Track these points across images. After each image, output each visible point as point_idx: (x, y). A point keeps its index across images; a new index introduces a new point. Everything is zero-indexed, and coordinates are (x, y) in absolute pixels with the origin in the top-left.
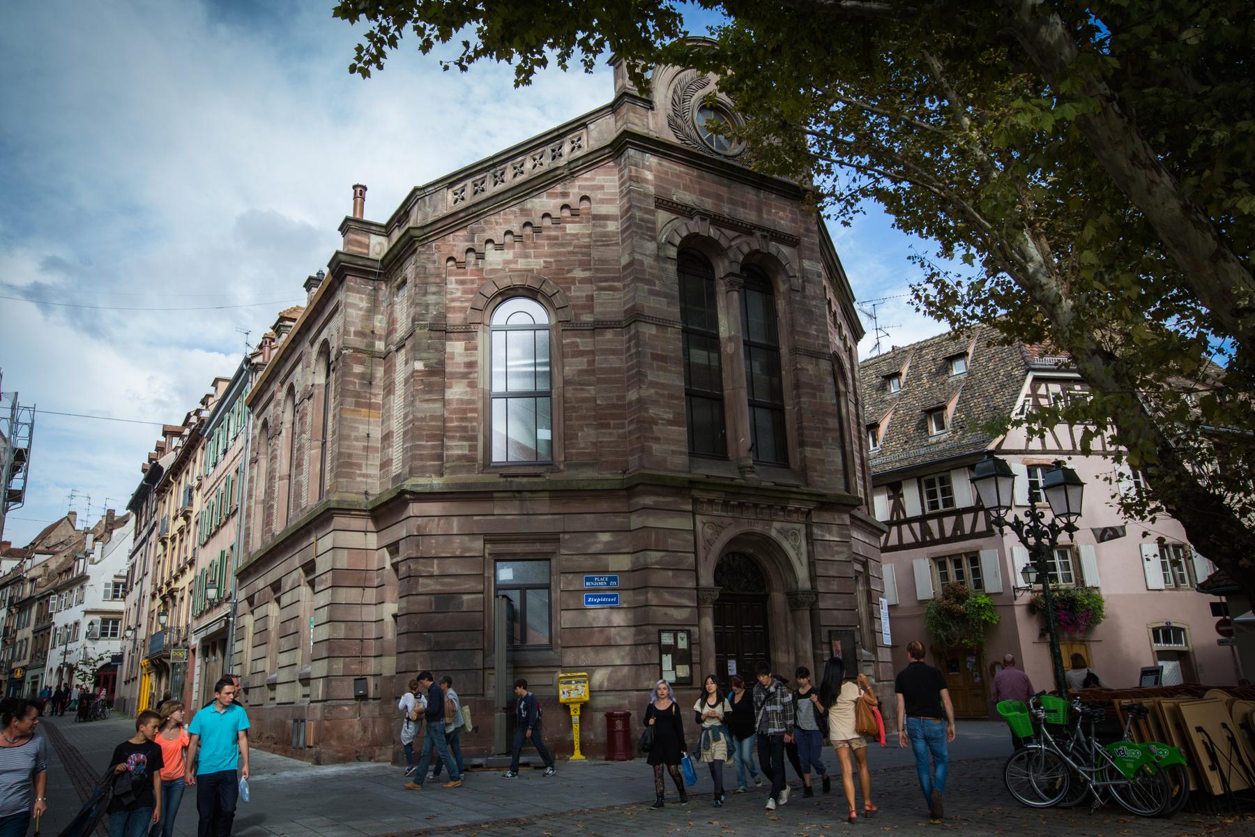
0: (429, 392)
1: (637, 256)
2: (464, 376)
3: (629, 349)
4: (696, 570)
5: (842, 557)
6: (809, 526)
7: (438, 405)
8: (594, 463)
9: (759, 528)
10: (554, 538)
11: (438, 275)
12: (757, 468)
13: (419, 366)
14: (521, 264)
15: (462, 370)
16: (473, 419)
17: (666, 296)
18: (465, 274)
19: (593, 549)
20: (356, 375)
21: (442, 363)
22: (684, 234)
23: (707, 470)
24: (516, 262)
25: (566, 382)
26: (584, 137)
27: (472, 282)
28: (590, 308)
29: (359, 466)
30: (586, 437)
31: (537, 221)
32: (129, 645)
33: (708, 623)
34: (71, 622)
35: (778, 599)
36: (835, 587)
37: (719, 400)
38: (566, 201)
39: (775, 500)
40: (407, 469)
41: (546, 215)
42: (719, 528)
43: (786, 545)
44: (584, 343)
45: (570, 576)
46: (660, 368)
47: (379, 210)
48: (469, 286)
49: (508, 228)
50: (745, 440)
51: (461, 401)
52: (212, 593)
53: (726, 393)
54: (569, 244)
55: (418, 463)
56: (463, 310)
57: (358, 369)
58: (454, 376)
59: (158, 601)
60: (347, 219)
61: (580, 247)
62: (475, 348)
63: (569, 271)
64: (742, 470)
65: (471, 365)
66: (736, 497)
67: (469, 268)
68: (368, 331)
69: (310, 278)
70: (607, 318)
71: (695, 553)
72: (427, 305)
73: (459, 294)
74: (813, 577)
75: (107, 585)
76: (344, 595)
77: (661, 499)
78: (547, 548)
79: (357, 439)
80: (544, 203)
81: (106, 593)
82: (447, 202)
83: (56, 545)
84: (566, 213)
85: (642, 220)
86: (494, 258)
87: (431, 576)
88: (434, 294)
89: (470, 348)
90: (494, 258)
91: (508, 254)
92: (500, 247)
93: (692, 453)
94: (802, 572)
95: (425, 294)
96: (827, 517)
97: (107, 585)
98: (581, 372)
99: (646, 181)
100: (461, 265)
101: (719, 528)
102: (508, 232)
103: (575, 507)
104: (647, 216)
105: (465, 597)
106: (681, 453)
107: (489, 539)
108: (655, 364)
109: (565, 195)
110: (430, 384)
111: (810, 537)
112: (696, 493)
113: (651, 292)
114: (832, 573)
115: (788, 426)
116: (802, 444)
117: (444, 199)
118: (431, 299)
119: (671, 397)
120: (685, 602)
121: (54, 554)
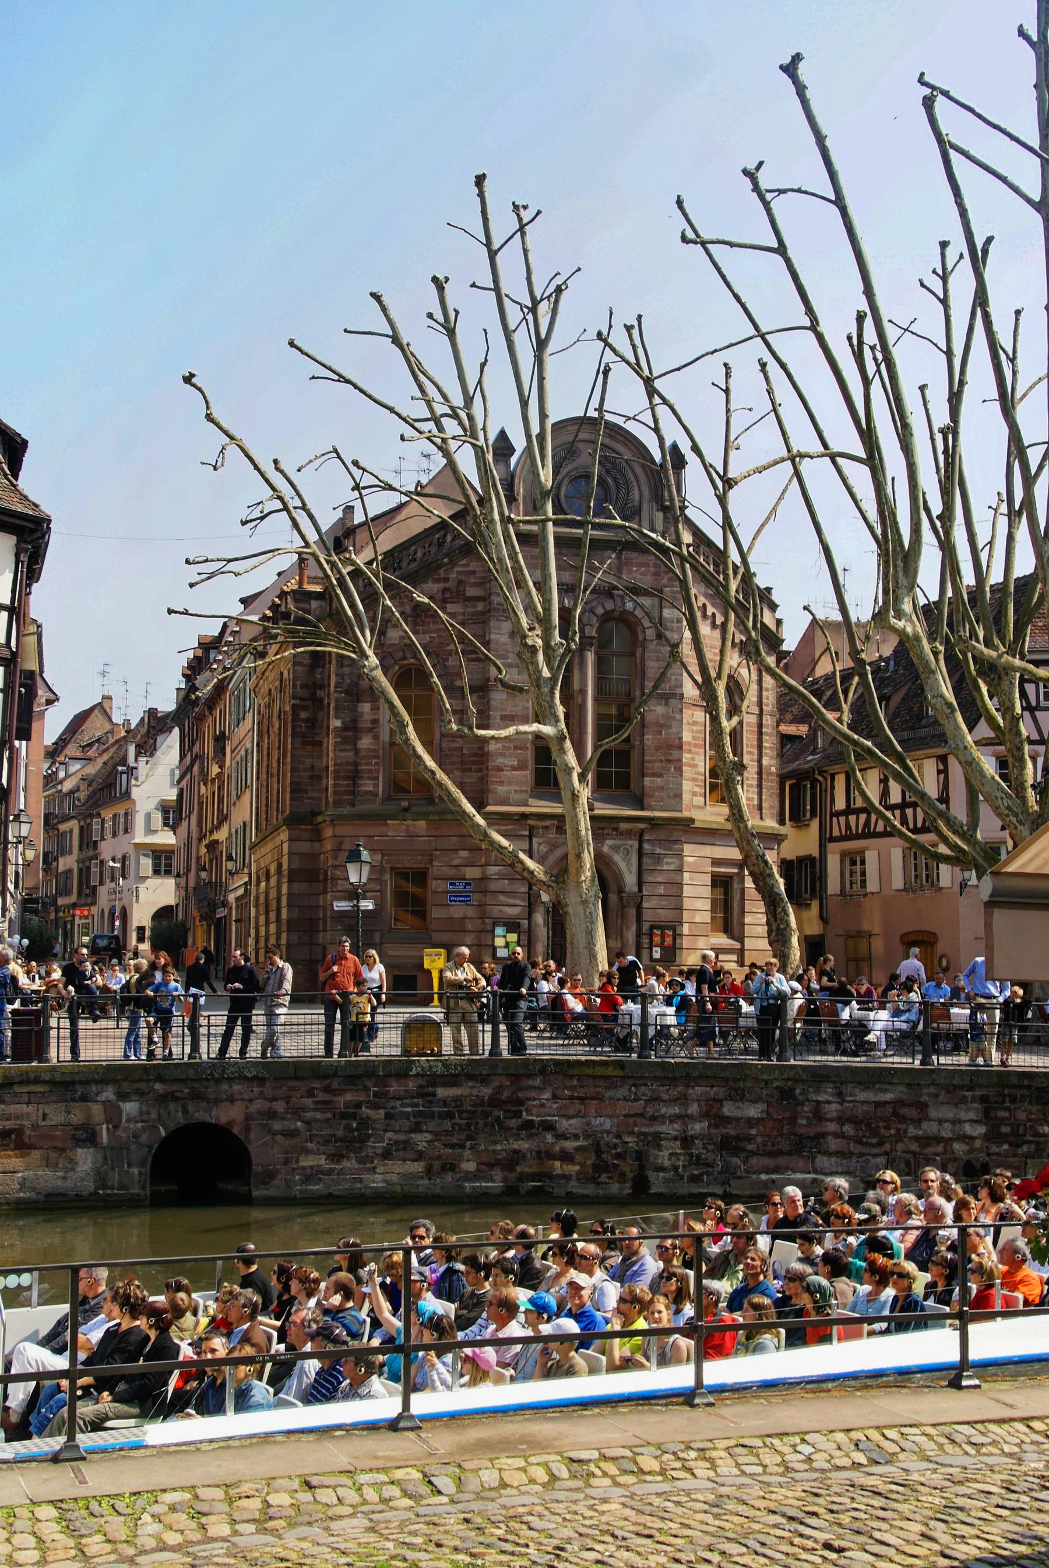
0: (346, 744)
2: (370, 730)
5: (672, 867)
6: (641, 843)
7: (351, 754)
15: (369, 725)
19: (456, 862)
20: (303, 720)
21: (354, 721)
29: (306, 791)
36: (661, 890)
57: (303, 715)
74: (640, 884)
79: (304, 770)
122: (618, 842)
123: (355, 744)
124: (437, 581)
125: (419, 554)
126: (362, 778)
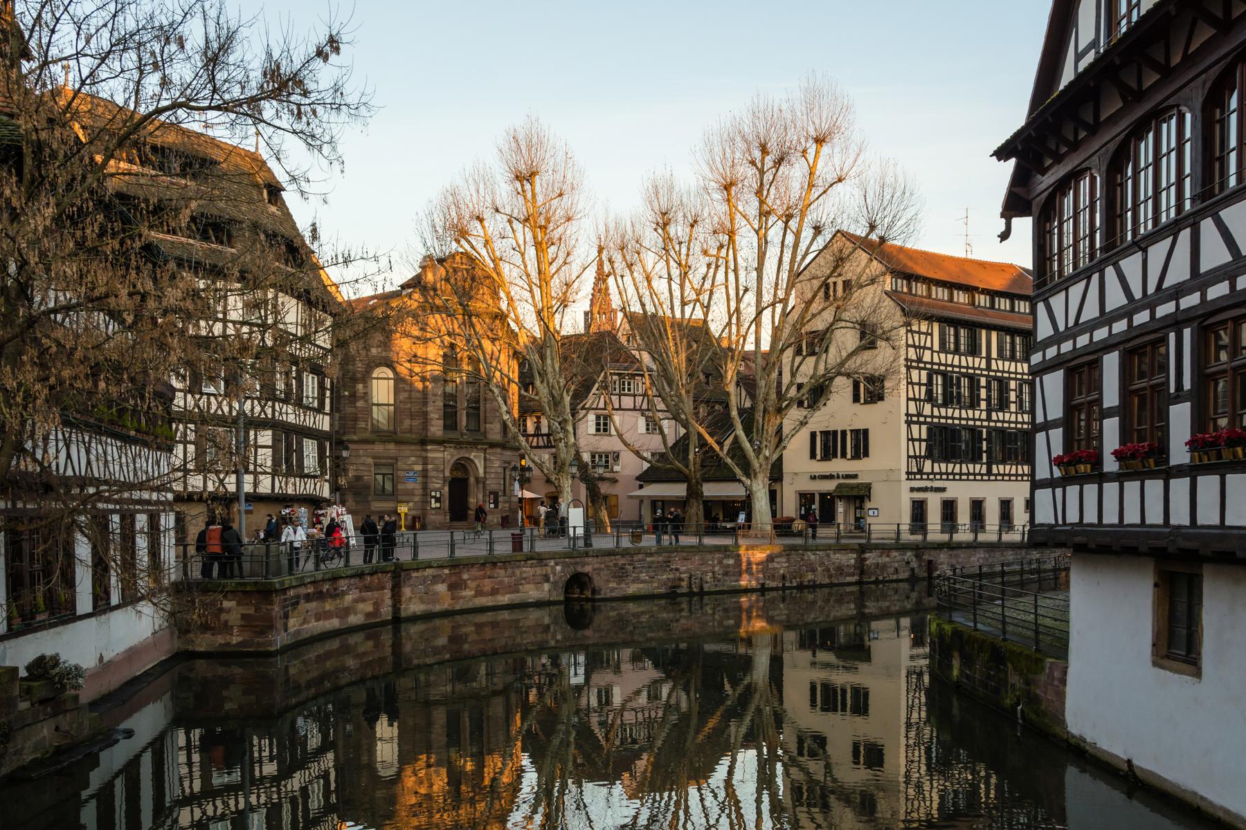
23: (452, 435)
33: (447, 489)
35: (472, 480)
39: (474, 445)
50: (464, 423)
66: (458, 444)
86: (374, 351)
89: (365, 387)
94: (481, 471)
96: (494, 450)
101: (452, 456)
103: (404, 447)
111: (485, 459)
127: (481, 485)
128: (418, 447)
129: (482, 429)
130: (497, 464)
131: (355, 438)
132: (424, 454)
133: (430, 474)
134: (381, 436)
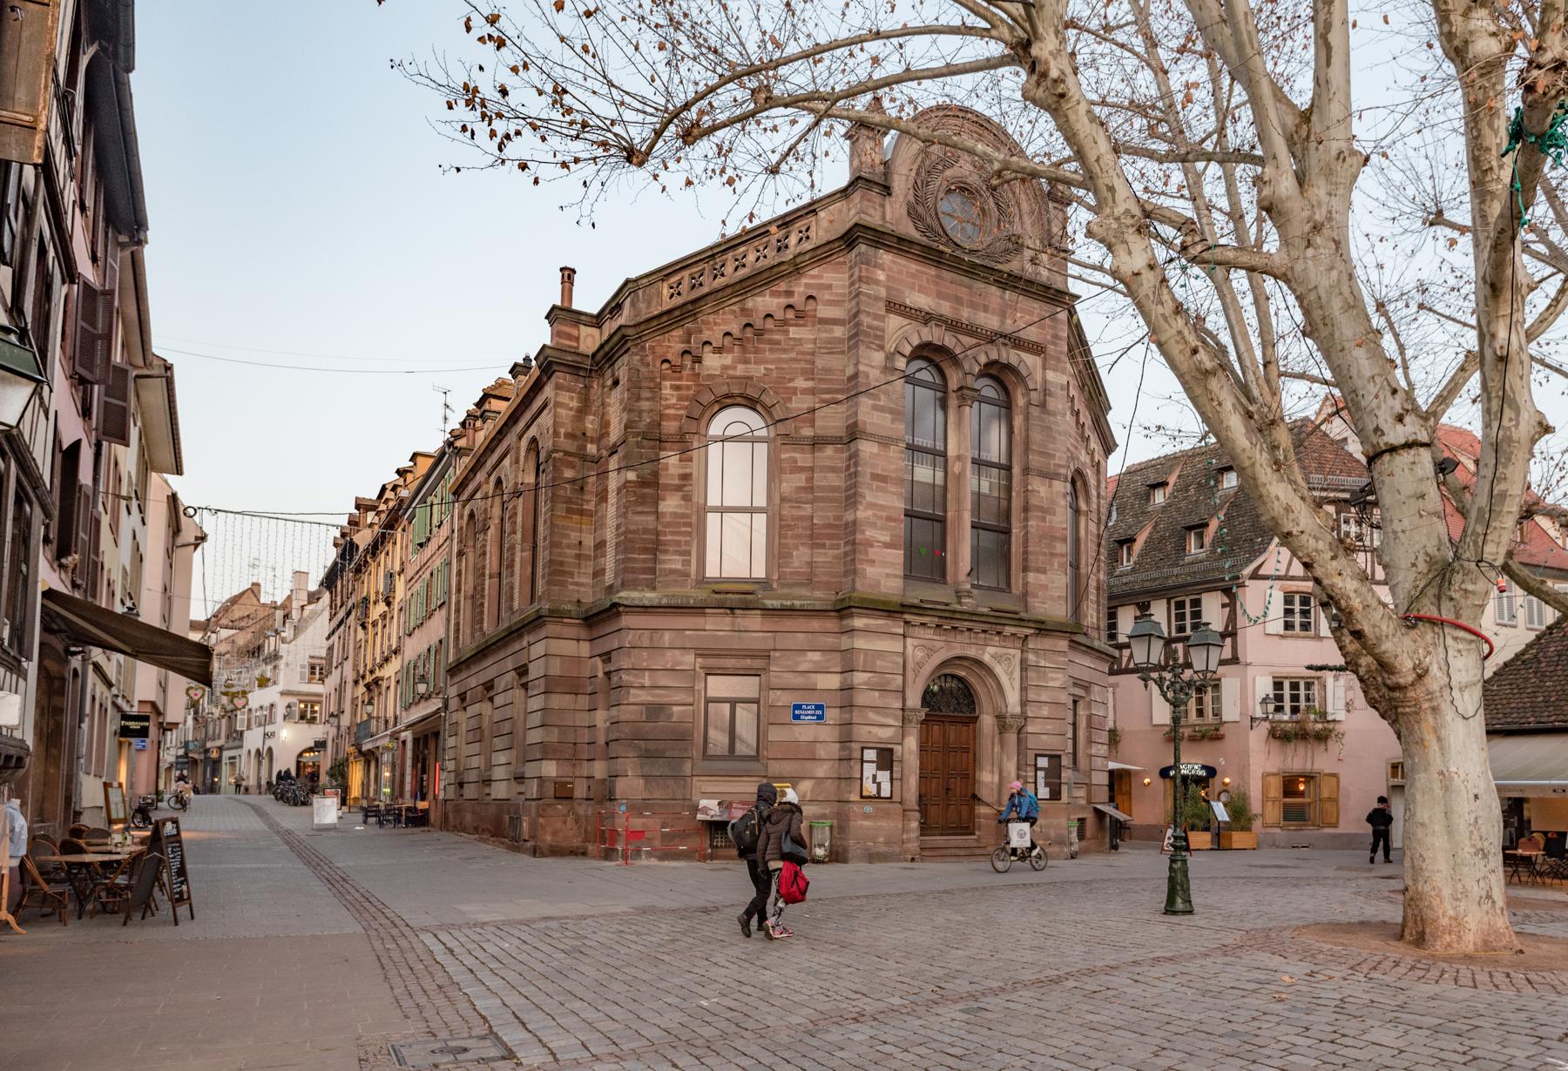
0: (642, 504)
1: (862, 368)
2: (679, 488)
3: (848, 468)
4: (903, 692)
5: (1057, 684)
7: (651, 518)
8: (810, 581)
9: (971, 652)
10: (766, 655)
11: (652, 380)
12: (975, 592)
13: (632, 476)
14: (740, 370)
15: (677, 482)
16: (690, 534)
17: (891, 411)
18: (680, 379)
21: (656, 474)
22: (916, 342)
24: (735, 368)
25: (783, 499)
26: (813, 229)
27: (688, 388)
28: (812, 423)
30: (801, 556)
31: (758, 323)
32: (333, 731)
33: (912, 743)
34: (266, 704)
35: (987, 721)
36: (1045, 712)
37: (942, 521)
38: (791, 301)
40: (619, 582)
41: (769, 316)
42: (931, 651)
43: (999, 670)
44: (803, 458)
45: (779, 693)
46: (879, 489)
47: (589, 299)
48: (684, 392)
49: (727, 328)
51: (675, 515)
52: (422, 688)
53: (949, 514)
54: (792, 350)
55: (630, 576)
56: (678, 418)
58: (667, 487)
59: (361, 689)
60: (554, 308)
61: (803, 353)
62: (691, 460)
63: (791, 380)
64: (959, 595)
65: (686, 477)
67: (686, 372)
68: (579, 433)
69: (516, 365)
70: (829, 433)
71: (904, 675)
72: (640, 412)
73: (674, 401)
75: (303, 666)
76: (557, 701)
77: (872, 622)
78: (758, 663)
80: (765, 302)
81: (302, 674)
82: (665, 298)
83: (242, 619)
84: (790, 314)
85: (869, 327)
86: (713, 362)
87: (643, 687)
88: (648, 399)
90: (712, 362)
91: (727, 359)
92: (719, 350)
93: (908, 576)
94: (1013, 698)
95: (639, 399)
97: (303, 666)
98: (799, 489)
99: (877, 282)
100: (676, 369)
101: (931, 651)
102: (728, 334)
103: (788, 624)
104: (875, 323)
105: (675, 709)
106: (895, 576)
107: (701, 653)
108: (875, 484)
109: (789, 293)
110: (643, 496)
111: (1024, 666)
112: (908, 617)
113: (875, 408)
114: (1043, 699)
115: (1013, 549)
116: (1025, 569)
117: (660, 294)
118: (645, 405)
119: (889, 519)
120: (891, 722)
121: (241, 629)
122: (1001, 651)
123: (657, 505)
124: (774, 294)
125: (751, 257)
126: (666, 552)
127: (1012, 737)
128: (831, 624)
129: (1017, 588)
130: (1057, 680)
131: (649, 597)
132: (845, 642)
133: (861, 699)
134: (736, 599)
